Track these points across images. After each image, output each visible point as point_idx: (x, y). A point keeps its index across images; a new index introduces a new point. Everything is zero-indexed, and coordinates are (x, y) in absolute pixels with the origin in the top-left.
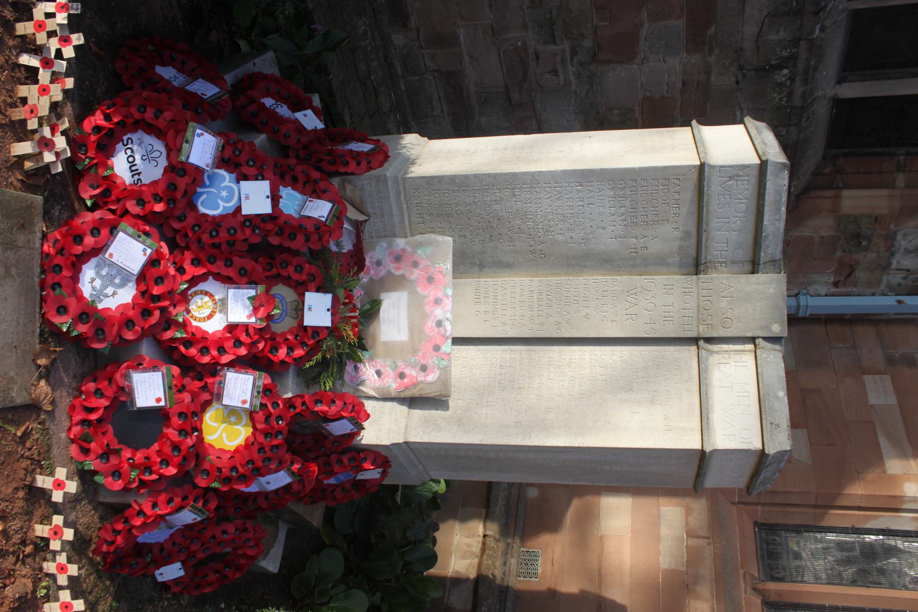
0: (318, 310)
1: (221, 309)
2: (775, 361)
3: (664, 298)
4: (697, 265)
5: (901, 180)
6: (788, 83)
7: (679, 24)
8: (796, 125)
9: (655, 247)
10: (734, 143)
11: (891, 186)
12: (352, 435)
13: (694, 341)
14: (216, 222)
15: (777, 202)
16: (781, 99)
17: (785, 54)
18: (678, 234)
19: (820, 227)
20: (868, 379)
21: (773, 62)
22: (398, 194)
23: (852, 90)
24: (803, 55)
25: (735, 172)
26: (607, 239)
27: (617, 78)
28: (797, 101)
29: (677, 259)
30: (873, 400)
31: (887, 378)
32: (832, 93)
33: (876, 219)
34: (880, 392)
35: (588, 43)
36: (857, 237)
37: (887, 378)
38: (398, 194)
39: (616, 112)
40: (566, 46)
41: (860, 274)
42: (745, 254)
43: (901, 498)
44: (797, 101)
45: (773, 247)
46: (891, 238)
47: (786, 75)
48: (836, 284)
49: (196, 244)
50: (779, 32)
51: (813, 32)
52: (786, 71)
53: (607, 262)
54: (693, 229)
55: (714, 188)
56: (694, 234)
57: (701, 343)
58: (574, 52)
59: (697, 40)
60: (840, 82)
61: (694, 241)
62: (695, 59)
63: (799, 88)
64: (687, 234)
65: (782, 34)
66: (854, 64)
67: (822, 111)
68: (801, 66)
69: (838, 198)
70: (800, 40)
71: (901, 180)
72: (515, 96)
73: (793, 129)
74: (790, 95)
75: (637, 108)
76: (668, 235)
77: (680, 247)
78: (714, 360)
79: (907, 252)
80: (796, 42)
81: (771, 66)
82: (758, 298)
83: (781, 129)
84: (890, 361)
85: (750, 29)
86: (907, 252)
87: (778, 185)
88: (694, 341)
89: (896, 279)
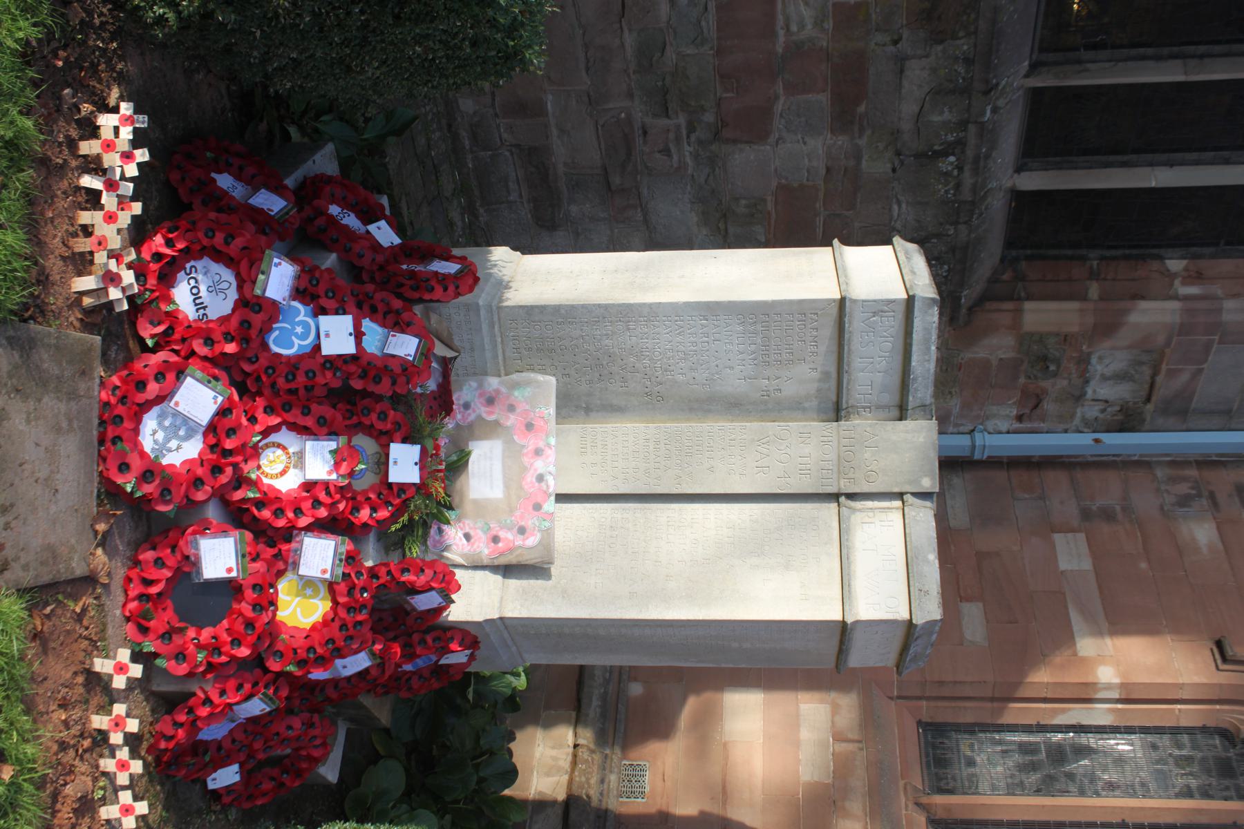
0: (404, 464)
1: (295, 464)
2: (924, 517)
3: (799, 449)
4: (837, 411)
5: (1094, 290)
6: (955, 172)
7: (822, 99)
8: (965, 223)
9: (790, 389)
10: (882, 272)
11: (1083, 298)
12: (439, 610)
13: (835, 497)
14: (293, 364)
15: (927, 341)
16: (947, 192)
17: (950, 138)
18: (815, 375)
19: (997, 347)
20: (1058, 538)
21: (936, 148)
22: (492, 325)
23: (1033, 181)
24: (972, 141)
25: (879, 307)
26: (735, 381)
27: (747, 165)
28: (966, 195)
29: (815, 403)
30: (1064, 565)
31: (1081, 537)
32: (1009, 184)
33: (1066, 338)
34: (1072, 555)
35: (709, 117)
36: (1043, 360)
37: (1081, 537)
38: (492, 325)
39: (743, 202)
40: (682, 120)
41: (1049, 406)
42: (891, 398)
43: (1093, 686)
44: (966, 195)
45: (922, 390)
46: (1084, 361)
47: (952, 163)
48: (1020, 418)
49: (272, 389)
50: (942, 113)
51: (983, 114)
52: (952, 159)
53: (734, 407)
54: (833, 369)
55: (856, 324)
56: (834, 375)
57: (842, 499)
58: (691, 129)
59: (844, 116)
60: (1019, 169)
61: (833, 383)
62: (842, 140)
63: (968, 179)
64: (826, 376)
65: (947, 116)
66: (1035, 149)
67: (997, 206)
68: (970, 153)
69: (1019, 312)
70: (968, 122)
71: (1094, 290)
72: (616, 180)
73: (962, 227)
74: (958, 186)
75: (769, 198)
76: (805, 375)
77: (819, 390)
78: (856, 519)
79: (1105, 378)
80: (963, 125)
81: (935, 152)
82: (907, 447)
83: (948, 227)
84: (1086, 515)
85: (909, 109)
86: (1105, 378)
87: (928, 322)
88: (835, 497)
89: (1092, 411)
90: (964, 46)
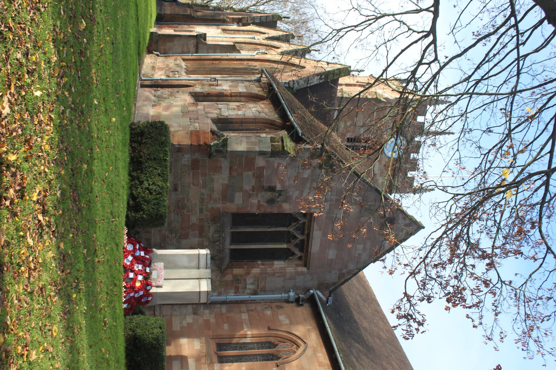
0: (148, 270)
1: (138, 267)
2: (210, 281)
3: (194, 273)
4: (199, 268)
5: (246, 267)
7: (197, 232)
10: (204, 252)
11: (244, 268)
12: (149, 290)
13: (198, 279)
14: (138, 256)
19: (229, 278)
20: (242, 314)
23: (233, 247)
25: (203, 255)
27: (184, 242)
28: (221, 249)
30: (243, 318)
31: (247, 314)
33: (241, 276)
34: (245, 316)
35: (179, 235)
36: (238, 280)
37: (247, 314)
40: (174, 235)
41: (240, 290)
43: (246, 335)
44: (221, 249)
45: (209, 266)
46: (245, 280)
48: (235, 293)
53: (186, 268)
55: (201, 257)
58: (176, 236)
59: (201, 235)
60: (230, 245)
62: (200, 239)
66: (233, 242)
67: (227, 251)
69: (232, 270)
71: (246, 267)
72: (162, 245)
76: (194, 264)
79: (250, 284)
80: (220, 237)
82: (207, 272)
84: (248, 310)
85: (211, 234)
86: (250, 284)
87: (209, 256)
88: (198, 279)
89: (248, 291)
90: (219, 225)
